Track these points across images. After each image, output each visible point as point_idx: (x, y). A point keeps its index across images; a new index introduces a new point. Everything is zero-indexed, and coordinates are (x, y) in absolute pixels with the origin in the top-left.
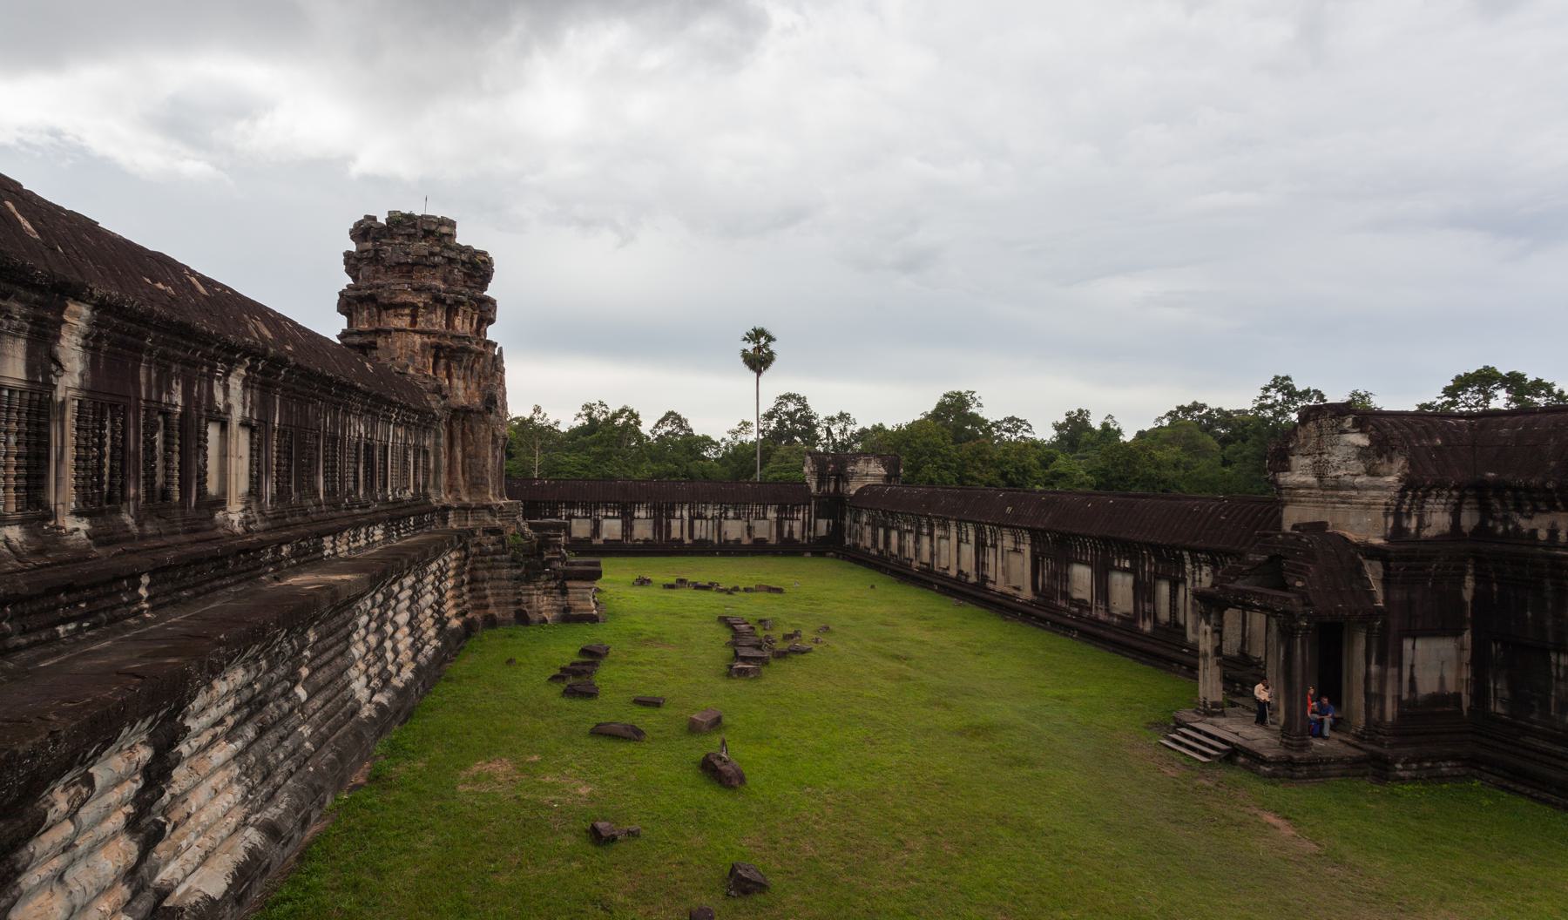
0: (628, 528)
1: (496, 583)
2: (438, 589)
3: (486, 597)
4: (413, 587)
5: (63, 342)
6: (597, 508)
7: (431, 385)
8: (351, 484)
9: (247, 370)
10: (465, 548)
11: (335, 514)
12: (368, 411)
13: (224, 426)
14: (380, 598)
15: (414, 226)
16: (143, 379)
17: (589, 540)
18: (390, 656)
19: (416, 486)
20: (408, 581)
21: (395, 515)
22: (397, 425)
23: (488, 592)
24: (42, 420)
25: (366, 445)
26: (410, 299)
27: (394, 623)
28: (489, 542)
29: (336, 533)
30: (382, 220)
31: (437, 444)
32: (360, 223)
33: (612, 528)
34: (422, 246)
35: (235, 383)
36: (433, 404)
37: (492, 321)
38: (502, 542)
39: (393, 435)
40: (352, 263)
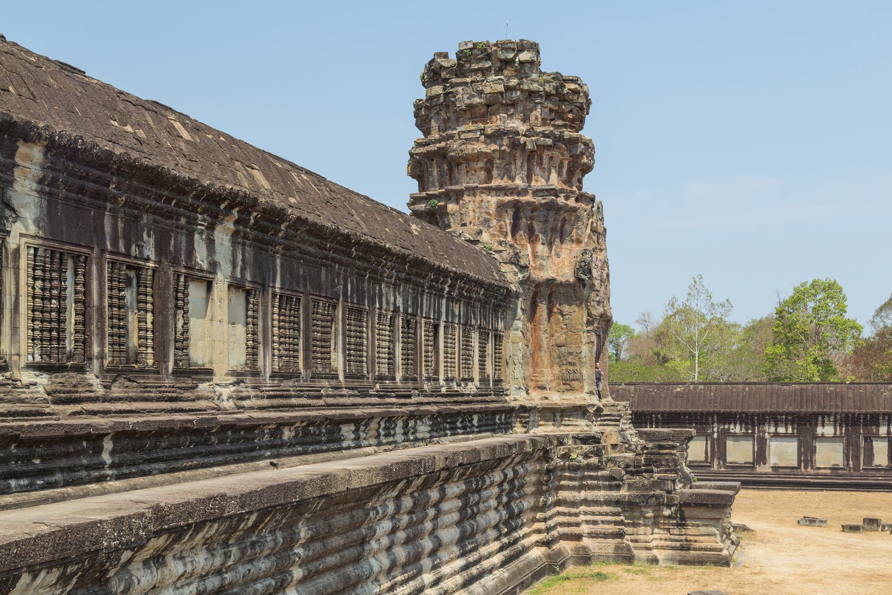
0: (807, 454)
2: (507, 506)
7: (507, 253)
10: (546, 456)
12: (407, 281)
14: (407, 502)
17: (751, 466)
20: (455, 489)
36: (510, 277)
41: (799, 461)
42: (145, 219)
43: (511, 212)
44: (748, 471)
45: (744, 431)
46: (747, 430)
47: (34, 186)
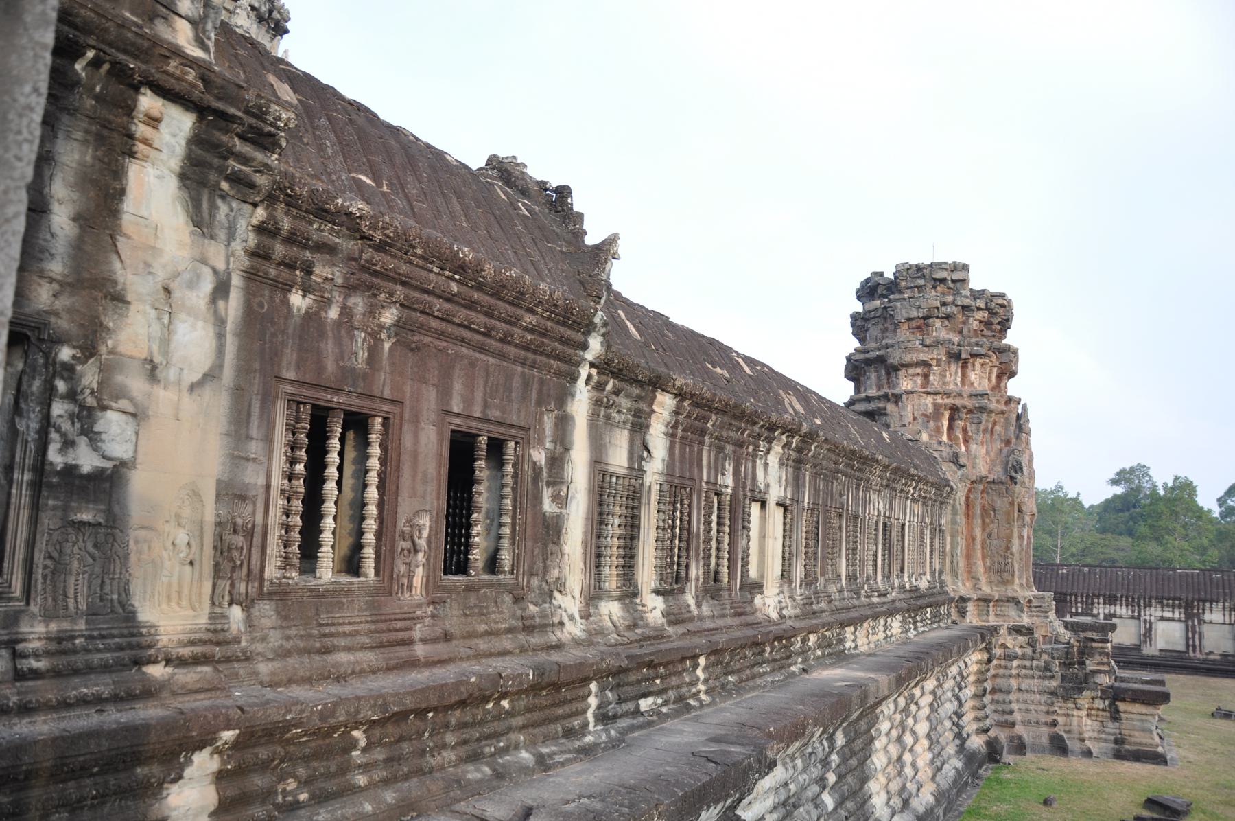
0: (1193, 636)
1: (1026, 696)
3: (1012, 712)
4: (933, 693)
5: (651, 430)
6: (1148, 605)
7: (946, 452)
8: (870, 569)
9: (784, 447)
10: (988, 649)
11: (856, 602)
12: (887, 486)
13: (763, 505)
14: (902, 702)
15: (923, 277)
16: (705, 462)
17: (1138, 648)
18: (908, 771)
19: (933, 572)
20: (930, 684)
21: (916, 604)
22: (914, 500)
23: (1015, 706)
24: (636, 503)
25: (885, 524)
26: (922, 357)
27: (913, 733)
28: (1015, 643)
29: (856, 622)
30: (889, 275)
31: (954, 522)
32: (867, 280)
33: (1168, 633)
34: (932, 298)
35: (773, 459)
37: (1013, 374)
38: (1032, 644)
39: (911, 513)
40: (860, 325)
41: (1188, 645)
42: (729, 449)
43: (947, 414)
44: (1134, 652)
45: (1130, 613)
46: (1133, 611)
47: (664, 429)
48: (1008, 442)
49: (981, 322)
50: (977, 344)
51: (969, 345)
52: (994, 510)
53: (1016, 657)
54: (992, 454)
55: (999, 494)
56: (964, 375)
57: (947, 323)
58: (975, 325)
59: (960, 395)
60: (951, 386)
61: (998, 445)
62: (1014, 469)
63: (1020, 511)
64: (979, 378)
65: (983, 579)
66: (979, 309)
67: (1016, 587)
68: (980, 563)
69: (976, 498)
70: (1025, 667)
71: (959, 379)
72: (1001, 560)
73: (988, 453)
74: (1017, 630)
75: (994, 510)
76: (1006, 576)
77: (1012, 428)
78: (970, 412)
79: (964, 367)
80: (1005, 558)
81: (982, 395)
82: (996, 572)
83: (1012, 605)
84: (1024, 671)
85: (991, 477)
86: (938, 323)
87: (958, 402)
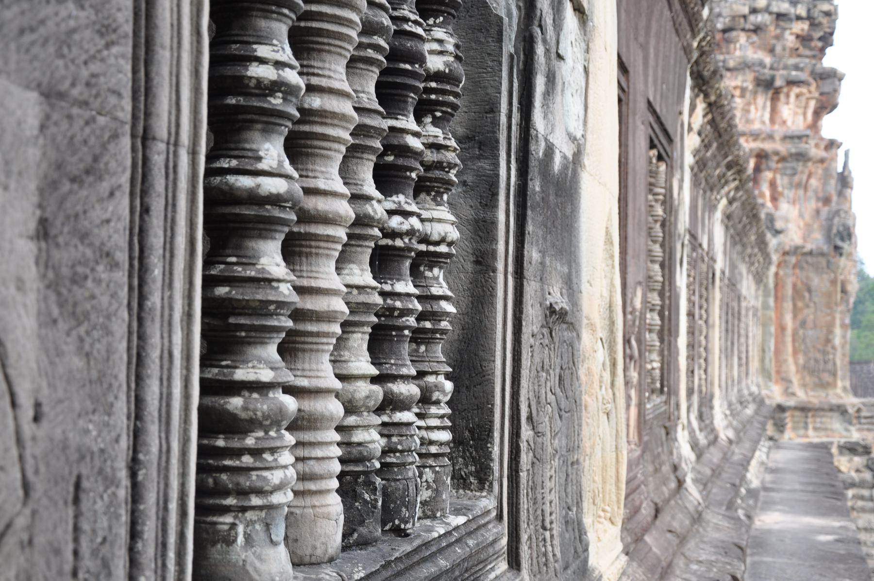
48: (827, 201)
49: (798, 36)
50: (796, 68)
51: (786, 67)
52: (809, 291)
53: (853, 485)
54: (807, 217)
55: (818, 269)
56: (774, 111)
57: (755, 38)
58: (790, 40)
59: (770, 137)
60: (757, 126)
61: (813, 204)
62: (840, 237)
63: (844, 291)
64: (793, 114)
65: (795, 380)
66: (799, 18)
67: (839, 391)
68: (790, 360)
69: (786, 275)
70: (862, 498)
71: (767, 116)
72: (819, 356)
73: (801, 215)
74: (851, 449)
75: (809, 291)
76: (826, 377)
77: (833, 182)
78: (783, 159)
79: (775, 99)
80: (825, 353)
81: (799, 137)
82: (812, 372)
83: (836, 415)
84: (860, 503)
85: (809, 247)
86: (742, 38)
87: (768, 146)
